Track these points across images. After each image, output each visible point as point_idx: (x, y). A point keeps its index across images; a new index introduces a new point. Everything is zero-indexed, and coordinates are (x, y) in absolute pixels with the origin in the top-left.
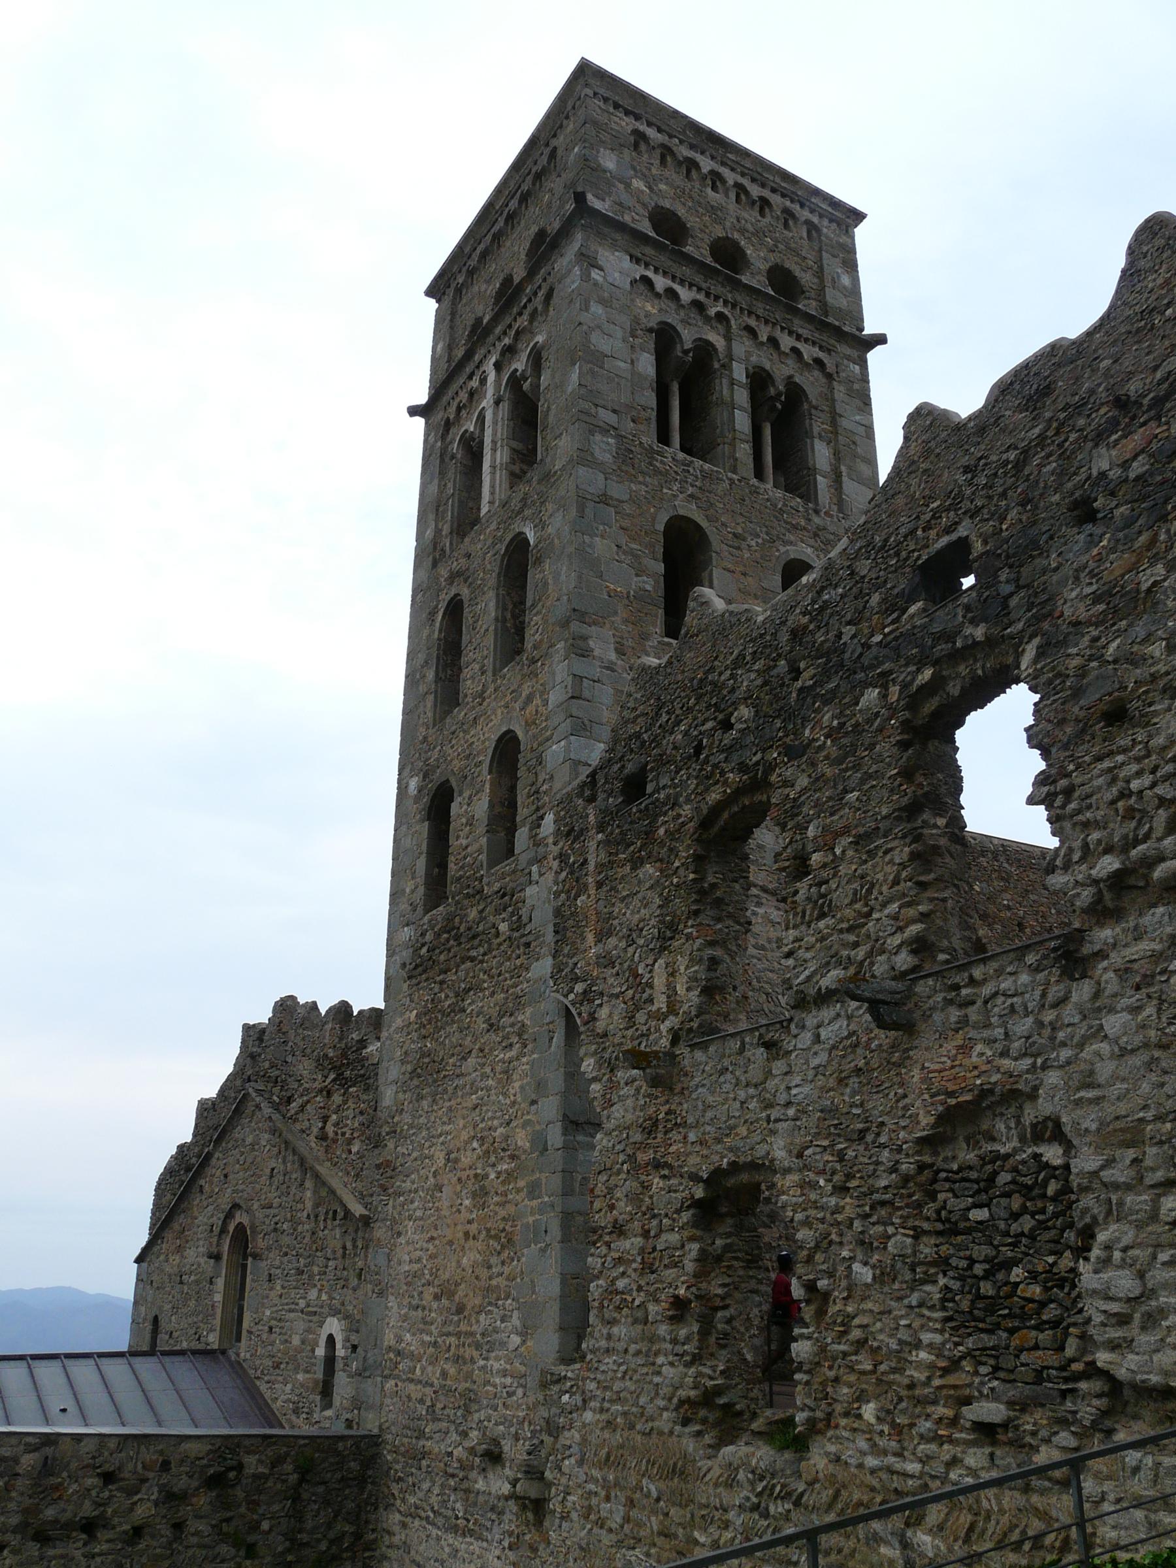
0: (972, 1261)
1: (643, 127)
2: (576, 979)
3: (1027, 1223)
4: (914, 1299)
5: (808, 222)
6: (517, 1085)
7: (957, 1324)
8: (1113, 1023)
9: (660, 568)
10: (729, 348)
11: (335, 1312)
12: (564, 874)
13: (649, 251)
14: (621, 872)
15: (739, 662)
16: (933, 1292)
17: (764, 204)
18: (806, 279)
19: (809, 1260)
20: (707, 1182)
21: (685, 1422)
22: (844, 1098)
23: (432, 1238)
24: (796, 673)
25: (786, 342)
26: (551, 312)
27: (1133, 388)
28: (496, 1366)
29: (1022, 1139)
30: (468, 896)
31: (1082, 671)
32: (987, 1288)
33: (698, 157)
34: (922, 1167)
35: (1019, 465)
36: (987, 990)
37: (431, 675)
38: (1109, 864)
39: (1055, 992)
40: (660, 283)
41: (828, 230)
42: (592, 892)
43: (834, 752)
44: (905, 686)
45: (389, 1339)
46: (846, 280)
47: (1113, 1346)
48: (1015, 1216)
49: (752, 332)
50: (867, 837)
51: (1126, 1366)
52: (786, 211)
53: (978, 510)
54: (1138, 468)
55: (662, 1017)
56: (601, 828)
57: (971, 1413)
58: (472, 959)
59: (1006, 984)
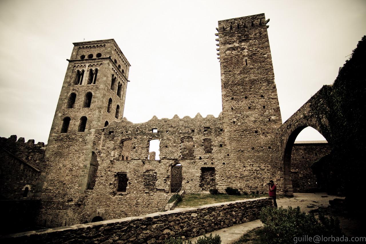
0: (147, 181)
1: (117, 49)
2: (97, 150)
3: (152, 179)
4: (141, 184)
5: (126, 65)
6: (81, 159)
7: (145, 185)
8: (162, 167)
9: (108, 104)
10: (118, 79)
12: (96, 138)
13: (114, 65)
14: (107, 141)
15: (130, 127)
16: (143, 183)
17: (123, 61)
18: (125, 71)
19: (130, 180)
20: (117, 173)
21: (110, 194)
22: (136, 168)
23: (58, 175)
24: (137, 131)
25: (122, 79)
26: (101, 66)
27: (173, 125)
28: (72, 190)
29: (152, 173)
30: (73, 134)
31: (165, 143)
32: (148, 183)
33: (120, 54)
34: (143, 174)
35: (163, 126)
36: (152, 162)
37: (66, 101)
38: (164, 156)
39: (158, 164)
40: (114, 69)
41: (128, 66)
42: (102, 141)
43: (140, 140)
44: (149, 137)
45: (44, 187)
46: (128, 73)
47: (158, 187)
48: (151, 178)
49: (120, 77)
50: (143, 148)
51: (158, 188)
52: (125, 63)
53: (159, 127)
54: (172, 131)
55: (113, 157)
56: (104, 135)
57: (145, 192)
58: (72, 142)
59: (154, 162)
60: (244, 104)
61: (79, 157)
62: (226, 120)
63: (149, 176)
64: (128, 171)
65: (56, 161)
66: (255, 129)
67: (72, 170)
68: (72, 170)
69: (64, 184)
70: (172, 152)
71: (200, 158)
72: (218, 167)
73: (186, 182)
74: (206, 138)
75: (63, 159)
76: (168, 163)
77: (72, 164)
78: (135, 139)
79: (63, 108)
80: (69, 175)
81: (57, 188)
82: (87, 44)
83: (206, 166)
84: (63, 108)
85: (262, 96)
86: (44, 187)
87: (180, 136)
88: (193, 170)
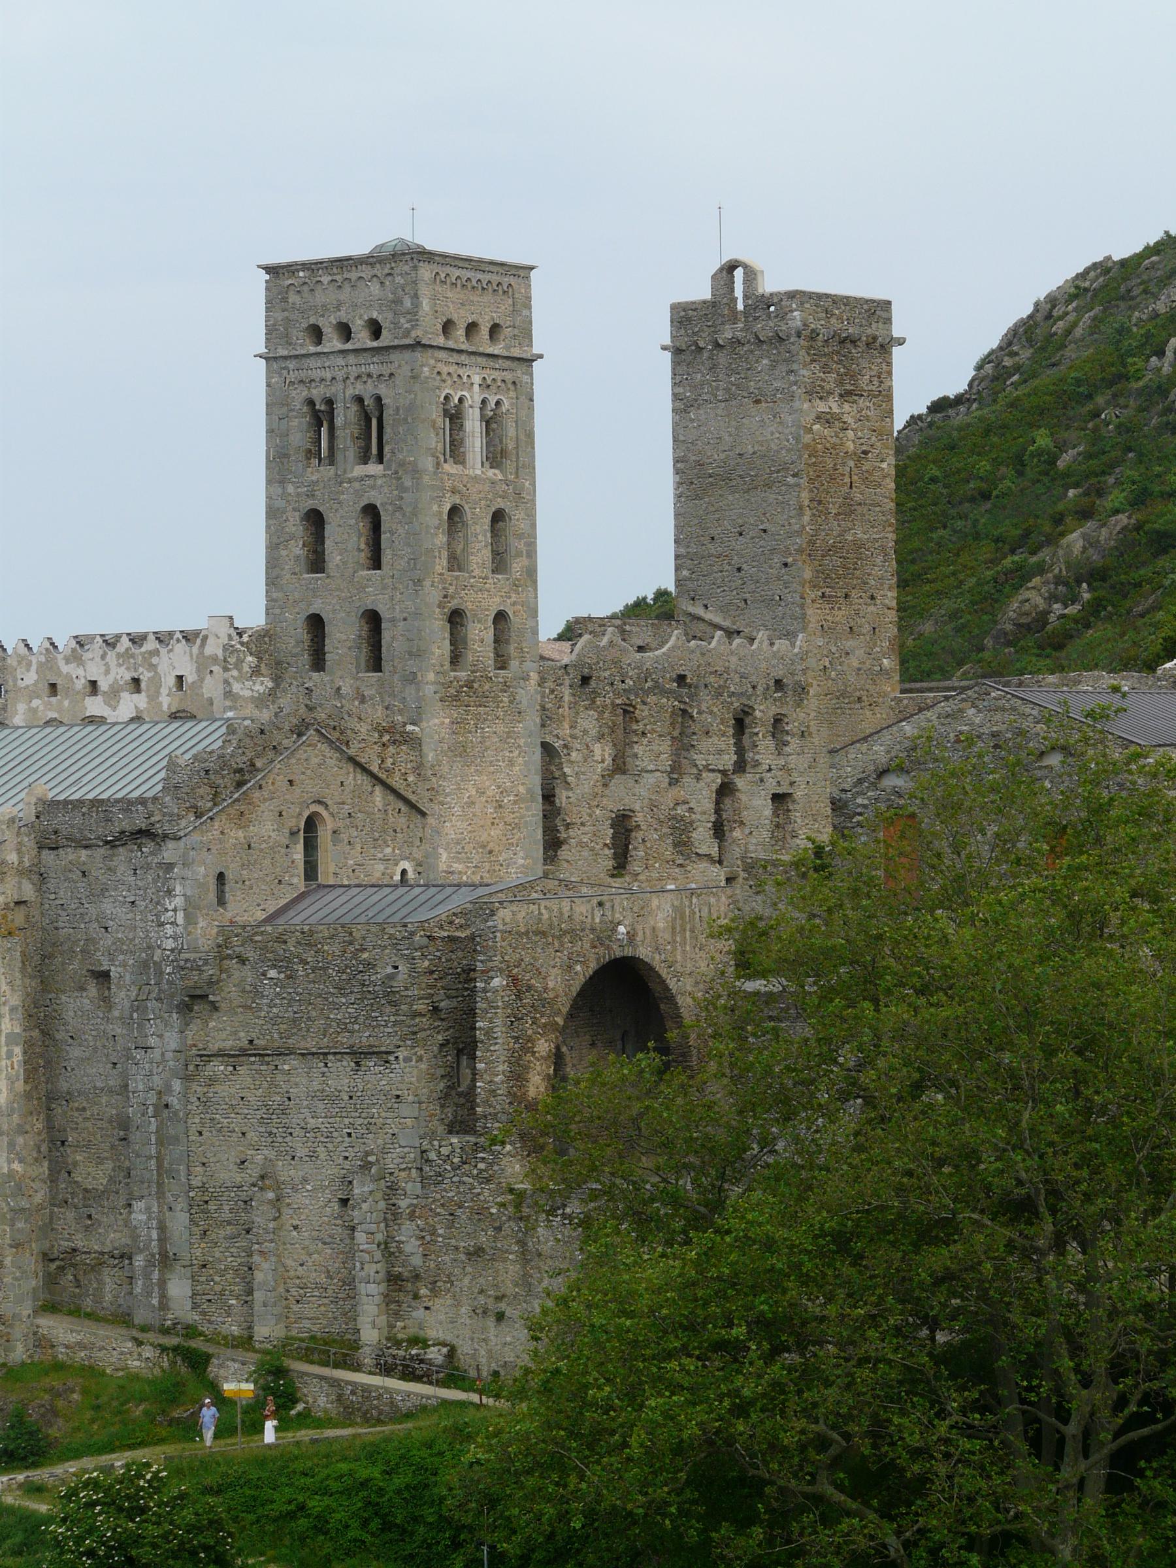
11: (407, 858)
15: (629, 665)
38: (704, 763)
45: (442, 867)
60: (841, 615)
61: (511, 763)
62: (812, 662)
63: (674, 818)
64: (637, 807)
65: (456, 776)
66: (858, 694)
67: (500, 806)
68: (500, 806)
69: (490, 852)
70: (720, 752)
71: (770, 770)
72: (799, 793)
73: (747, 832)
74: (779, 711)
75: (473, 769)
76: (713, 781)
77: (499, 787)
78: (643, 707)
79: (439, 569)
80: (496, 821)
81: (476, 867)
82: (457, 263)
83: (780, 791)
84: (439, 569)
85: (872, 598)
86: (442, 867)
87: (732, 704)
88: (760, 802)
